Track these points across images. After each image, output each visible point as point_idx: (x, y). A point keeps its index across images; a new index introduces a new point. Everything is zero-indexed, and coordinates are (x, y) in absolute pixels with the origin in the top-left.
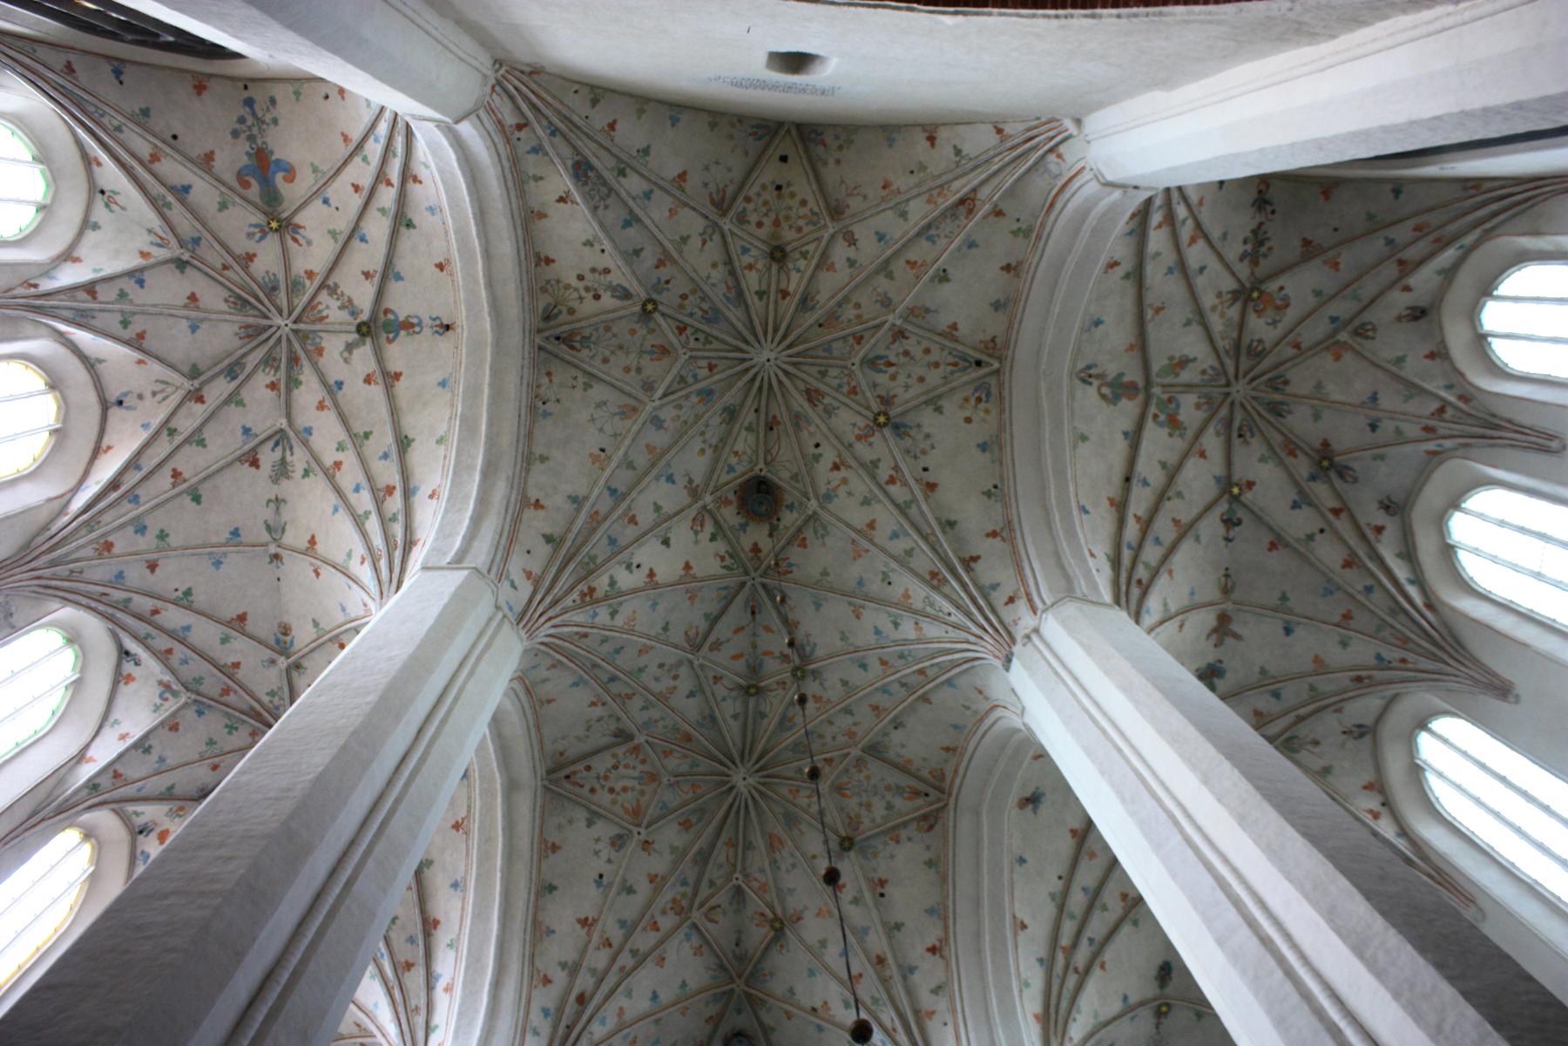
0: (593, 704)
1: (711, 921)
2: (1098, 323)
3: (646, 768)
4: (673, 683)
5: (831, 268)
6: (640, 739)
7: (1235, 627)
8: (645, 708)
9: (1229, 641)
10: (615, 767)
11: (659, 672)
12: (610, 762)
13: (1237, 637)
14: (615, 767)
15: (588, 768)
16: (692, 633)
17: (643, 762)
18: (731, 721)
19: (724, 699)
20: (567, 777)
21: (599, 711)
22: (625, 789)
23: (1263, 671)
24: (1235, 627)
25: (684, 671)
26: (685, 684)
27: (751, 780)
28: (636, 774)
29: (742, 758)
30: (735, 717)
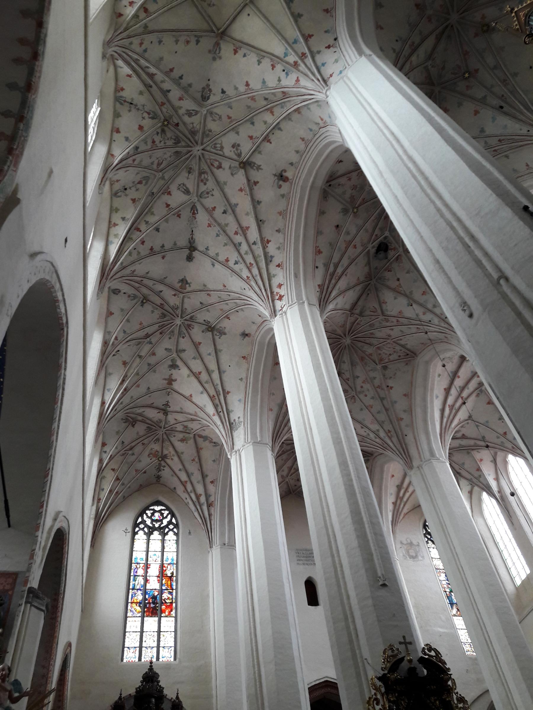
0: (391, 388)
1: (375, 308)
2: (214, 461)
3: (379, 352)
4: (363, 385)
5: (288, 467)
6: (379, 367)
7: (166, 382)
8: (375, 378)
9: (167, 377)
10: (390, 355)
11: (367, 393)
12: (391, 358)
13: (165, 379)
14: (390, 355)
15: (399, 356)
16: (353, 401)
17: (380, 354)
18: (346, 361)
19: (347, 371)
20: (408, 355)
21: (391, 383)
22: (389, 348)
23: (155, 371)
24: (166, 382)
25: (359, 389)
26: (359, 382)
27: (344, 341)
28: (384, 351)
29: (346, 346)
30: (344, 362)
